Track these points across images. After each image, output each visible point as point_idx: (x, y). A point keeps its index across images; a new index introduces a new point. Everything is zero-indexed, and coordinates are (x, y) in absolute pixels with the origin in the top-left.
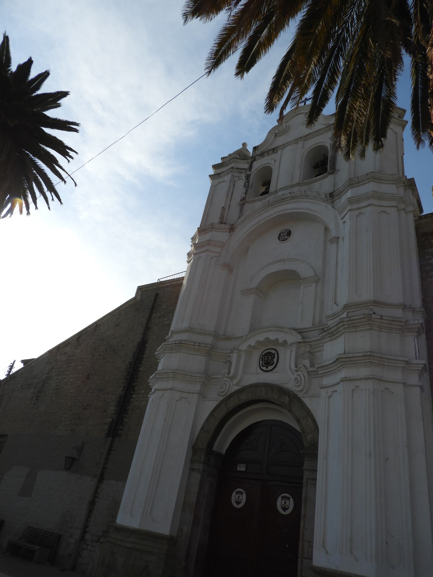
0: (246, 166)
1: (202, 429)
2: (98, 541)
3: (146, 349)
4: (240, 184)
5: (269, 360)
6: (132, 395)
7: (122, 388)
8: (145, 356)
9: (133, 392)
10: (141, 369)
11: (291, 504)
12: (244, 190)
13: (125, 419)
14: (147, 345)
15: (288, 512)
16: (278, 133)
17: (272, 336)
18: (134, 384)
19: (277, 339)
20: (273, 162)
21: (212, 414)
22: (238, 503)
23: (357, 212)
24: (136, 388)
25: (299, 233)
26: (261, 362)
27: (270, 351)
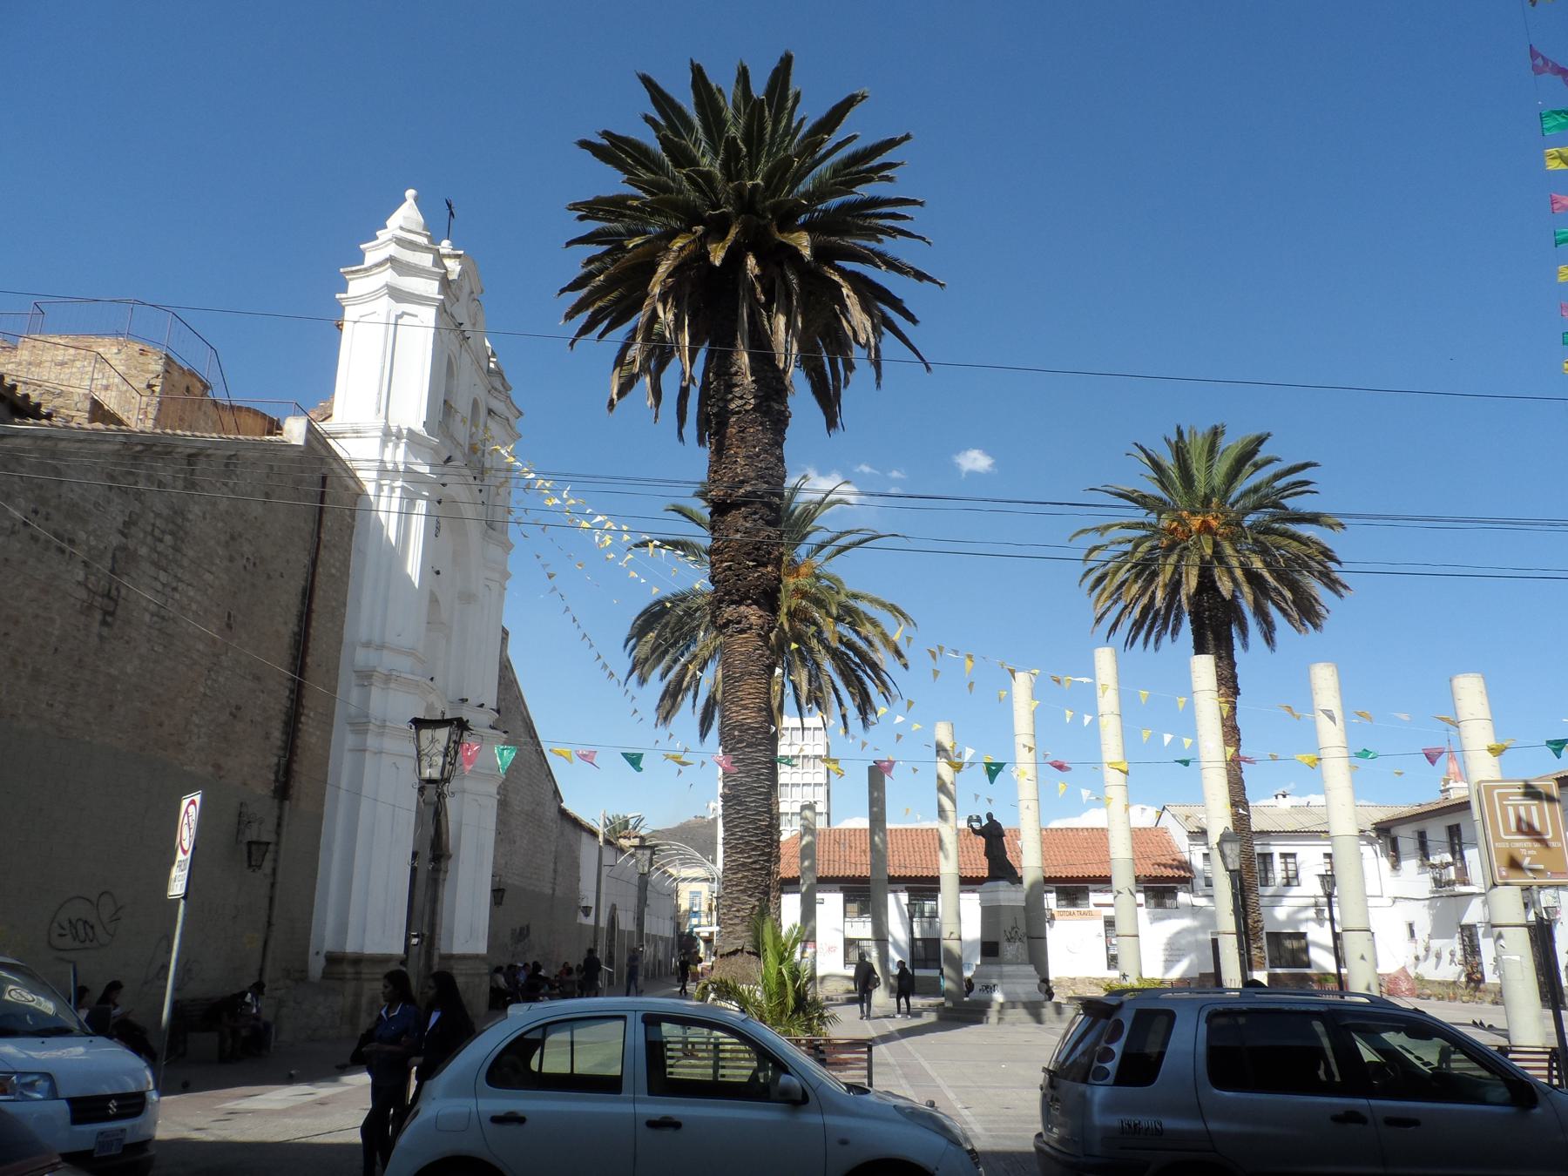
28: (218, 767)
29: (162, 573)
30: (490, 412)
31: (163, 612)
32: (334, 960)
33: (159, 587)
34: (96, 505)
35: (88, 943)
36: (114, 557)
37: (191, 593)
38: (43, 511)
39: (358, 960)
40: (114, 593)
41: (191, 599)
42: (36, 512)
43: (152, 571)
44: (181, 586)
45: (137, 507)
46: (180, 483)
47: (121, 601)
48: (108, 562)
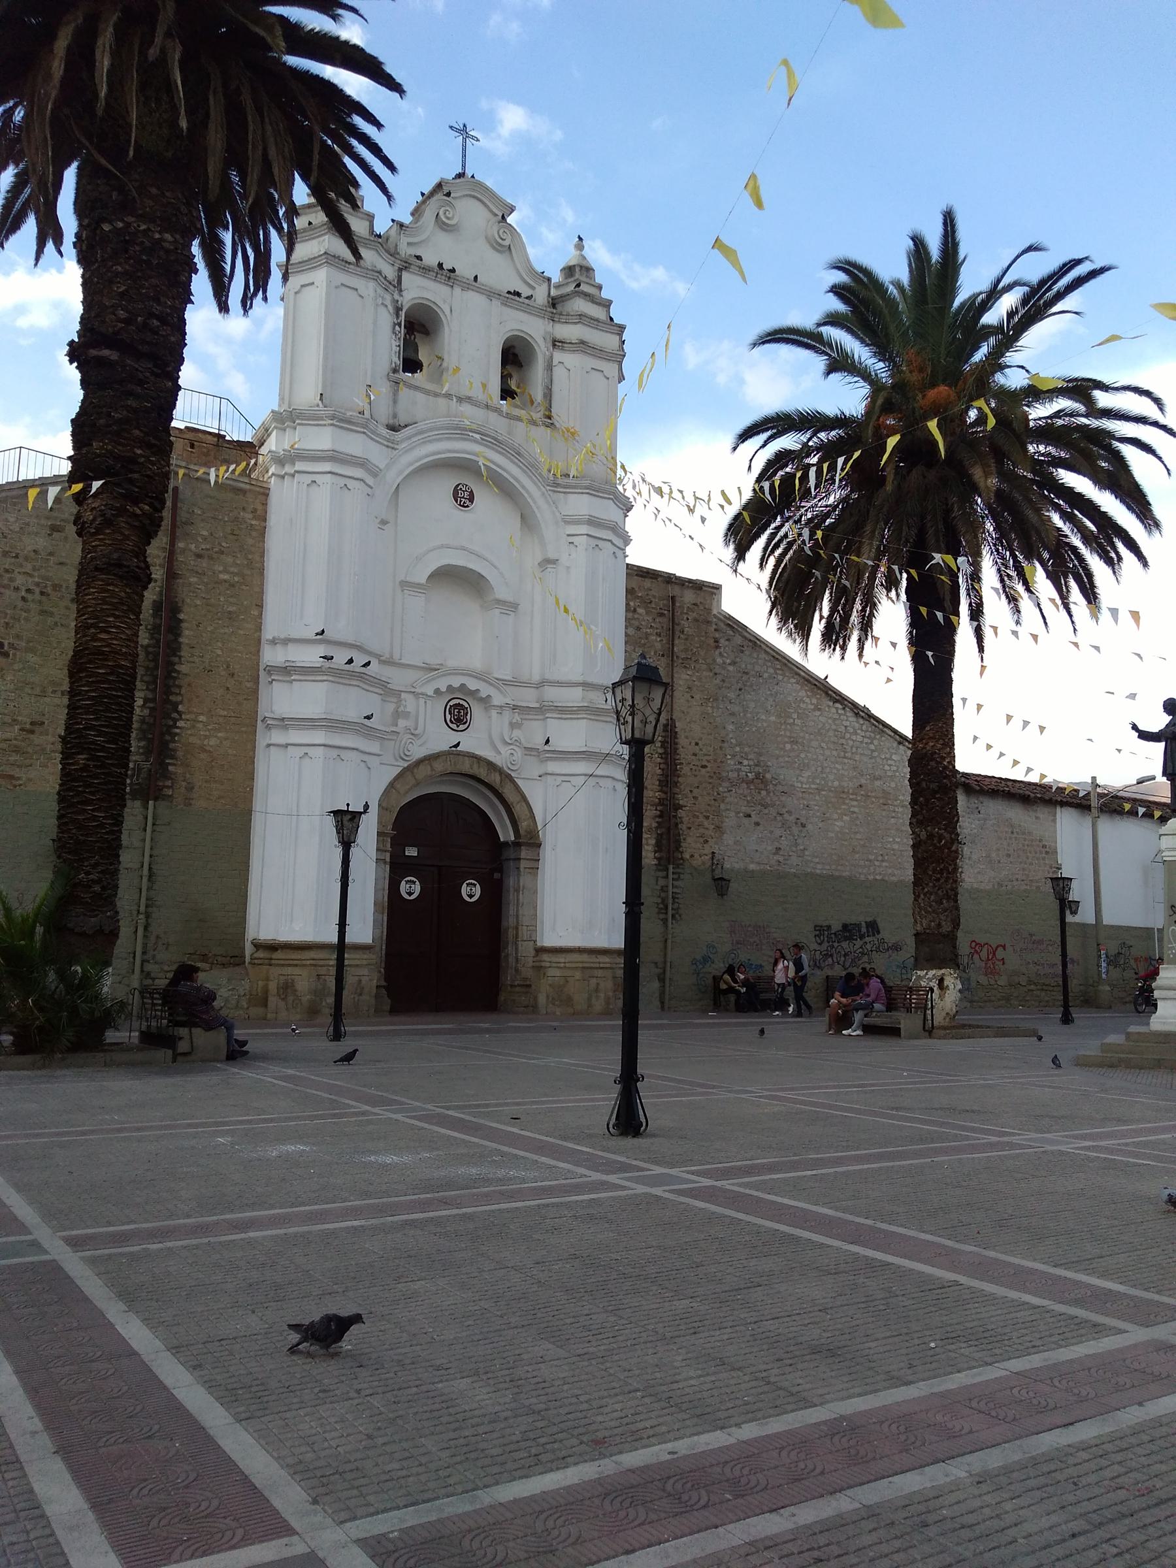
0: (390, 272)
3: (184, 625)
4: (386, 319)
5: (458, 716)
6: (175, 721)
8: (181, 640)
9: (175, 715)
10: (183, 668)
11: (477, 891)
12: (395, 343)
13: (170, 768)
14: (181, 616)
15: (473, 900)
16: (444, 223)
17: (472, 685)
18: (172, 698)
19: (478, 690)
21: (391, 785)
22: (410, 894)
23: (594, 542)
25: (485, 499)
26: (448, 717)
27: (462, 702)
28: (11, 777)
30: (556, 343)
32: (258, 945)
39: (273, 947)
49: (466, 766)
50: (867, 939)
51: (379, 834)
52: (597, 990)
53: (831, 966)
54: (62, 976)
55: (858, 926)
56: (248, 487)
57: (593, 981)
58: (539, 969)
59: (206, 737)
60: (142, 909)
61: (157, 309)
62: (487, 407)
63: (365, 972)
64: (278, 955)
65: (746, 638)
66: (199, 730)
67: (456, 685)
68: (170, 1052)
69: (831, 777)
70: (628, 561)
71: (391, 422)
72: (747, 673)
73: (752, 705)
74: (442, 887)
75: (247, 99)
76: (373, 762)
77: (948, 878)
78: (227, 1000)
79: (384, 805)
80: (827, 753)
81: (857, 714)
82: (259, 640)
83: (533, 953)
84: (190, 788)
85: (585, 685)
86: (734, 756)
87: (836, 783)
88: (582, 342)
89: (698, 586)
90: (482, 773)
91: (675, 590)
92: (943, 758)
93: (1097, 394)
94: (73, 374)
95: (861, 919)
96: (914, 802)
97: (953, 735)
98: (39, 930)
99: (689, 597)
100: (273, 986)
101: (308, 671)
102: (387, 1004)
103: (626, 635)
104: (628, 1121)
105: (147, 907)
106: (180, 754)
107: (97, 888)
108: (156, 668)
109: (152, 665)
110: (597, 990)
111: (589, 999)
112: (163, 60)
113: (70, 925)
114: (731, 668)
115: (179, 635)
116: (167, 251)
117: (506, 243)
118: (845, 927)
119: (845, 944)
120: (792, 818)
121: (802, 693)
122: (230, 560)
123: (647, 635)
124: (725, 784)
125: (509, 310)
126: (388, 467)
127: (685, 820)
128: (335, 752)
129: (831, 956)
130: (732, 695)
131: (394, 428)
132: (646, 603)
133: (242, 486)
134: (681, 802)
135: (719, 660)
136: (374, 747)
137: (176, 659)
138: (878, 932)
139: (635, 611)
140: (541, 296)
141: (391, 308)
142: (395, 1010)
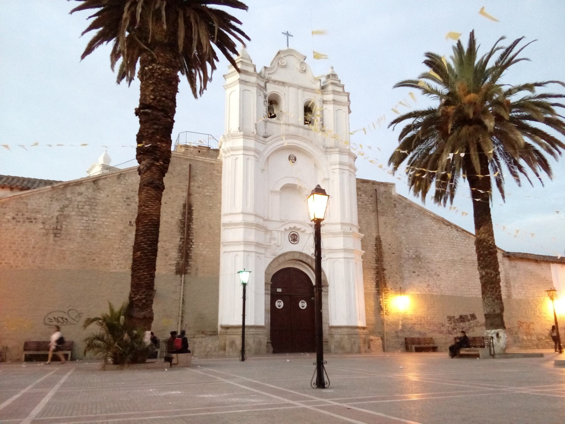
0: (262, 84)
1: (265, 273)
2: (194, 337)
3: (194, 211)
4: (262, 100)
5: (294, 238)
6: (191, 245)
7: (179, 239)
9: (191, 243)
10: (194, 226)
11: (305, 305)
17: (298, 226)
19: (300, 229)
20: (283, 94)
21: (270, 265)
22: (279, 306)
23: (342, 171)
24: (193, 241)
29: (85, 218)
30: (324, 102)
31: (88, 228)
33: (84, 221)
34: (45, 206)
35: (65, 323)
36: (57, 218)
37: (104, 220)
38: (20, 214)
39: (227, 328)
40: (59, 227)
41: (104, 222)
42: (17, 215)
43: (80, 218)
44: (97, 219)
45: (67, 202)
46: (91, 190)
47: (63, 229)
48: (55, 220)
49: (297, 257)
50: (471, 322)
51: (266, 284)
52: (355, 343)
53: (456, 333)
54: (130, 334)
55: (466, 316)
56: (215, 162)
57: (353, 340)
58: (331, 335)
59: (203, 251)
60: (180, 314)
61: (164, 94)
62: (299, 127)
63: (262, 337)
64: (229, 330)
65: (407, 203)
66: (199, 248)
67: (292, 226)
68: (169, 363)
69: (449, 256)
70: (357, 177)
71: (264, 135)
72: (408, 216)
73: (412, 229)
74: (291, 303)
75: (192, 20)
76: (262, 256)
77: (496, 291)
78: (211, 348)
79: (268, 272)
80: (446, 246)
81: (457, 230)
82: (220, 216)
83: (328, 328)
84: (197, 269)
85: (342, 224)
86: (406, 249)
87: (451, 258)
88: (334, 100)
89: (385, 185)
90: (304, 259)
91: (376, 187)
92: (489, 241)
93: (536, 88)
94: (137, 119)
95: (467, 313)
96: (479, 259)
97: (493, 231)
98: (122, 318)
99: (382, 189)
100: (227, 343)
101: (236, 224)
102: (271, 349)
103: (358, 205)
104: (321, 383)
105: (182, 314)
106: (193, 257)
107: (144, 301)
108: (184, 227)
109: (183, 226)
110: (355, 343)
111: (352, 346)
112: (159, 10)
113: (134, 315)
114: (402, 215)
115: (192, 215)
116: (168, 74)
117: (304, 69)
118: (461, 317)
119: (462, 324)
120: (433, 273)
121: (433, 223)
122: (209, 188)
123: (366, 205)
124: (403, 260)
125: (306, 93)
126: (264, 151)
127: (387, 275)
128: (247, 253)
129: (456, 329)
130: (403, 225)
131: (265, 137)
132: (365, 192)
133: (213, 162)
134: (385, 268)
135: (396, 212)
136: (262, 251)
137: (191, 224)
138: (476, 318)
139: (361, 195)
140: (317, 86)
141: (263, 97)
142: (275, 352)
